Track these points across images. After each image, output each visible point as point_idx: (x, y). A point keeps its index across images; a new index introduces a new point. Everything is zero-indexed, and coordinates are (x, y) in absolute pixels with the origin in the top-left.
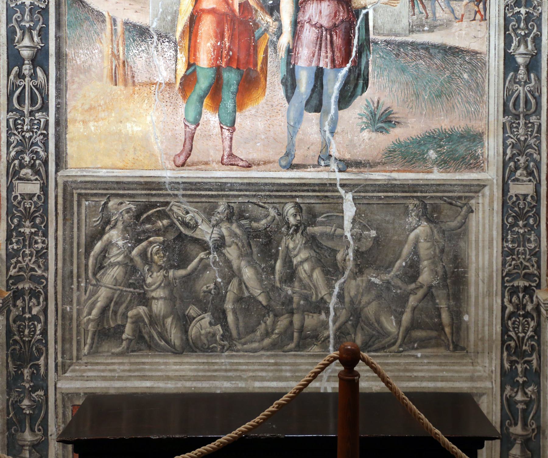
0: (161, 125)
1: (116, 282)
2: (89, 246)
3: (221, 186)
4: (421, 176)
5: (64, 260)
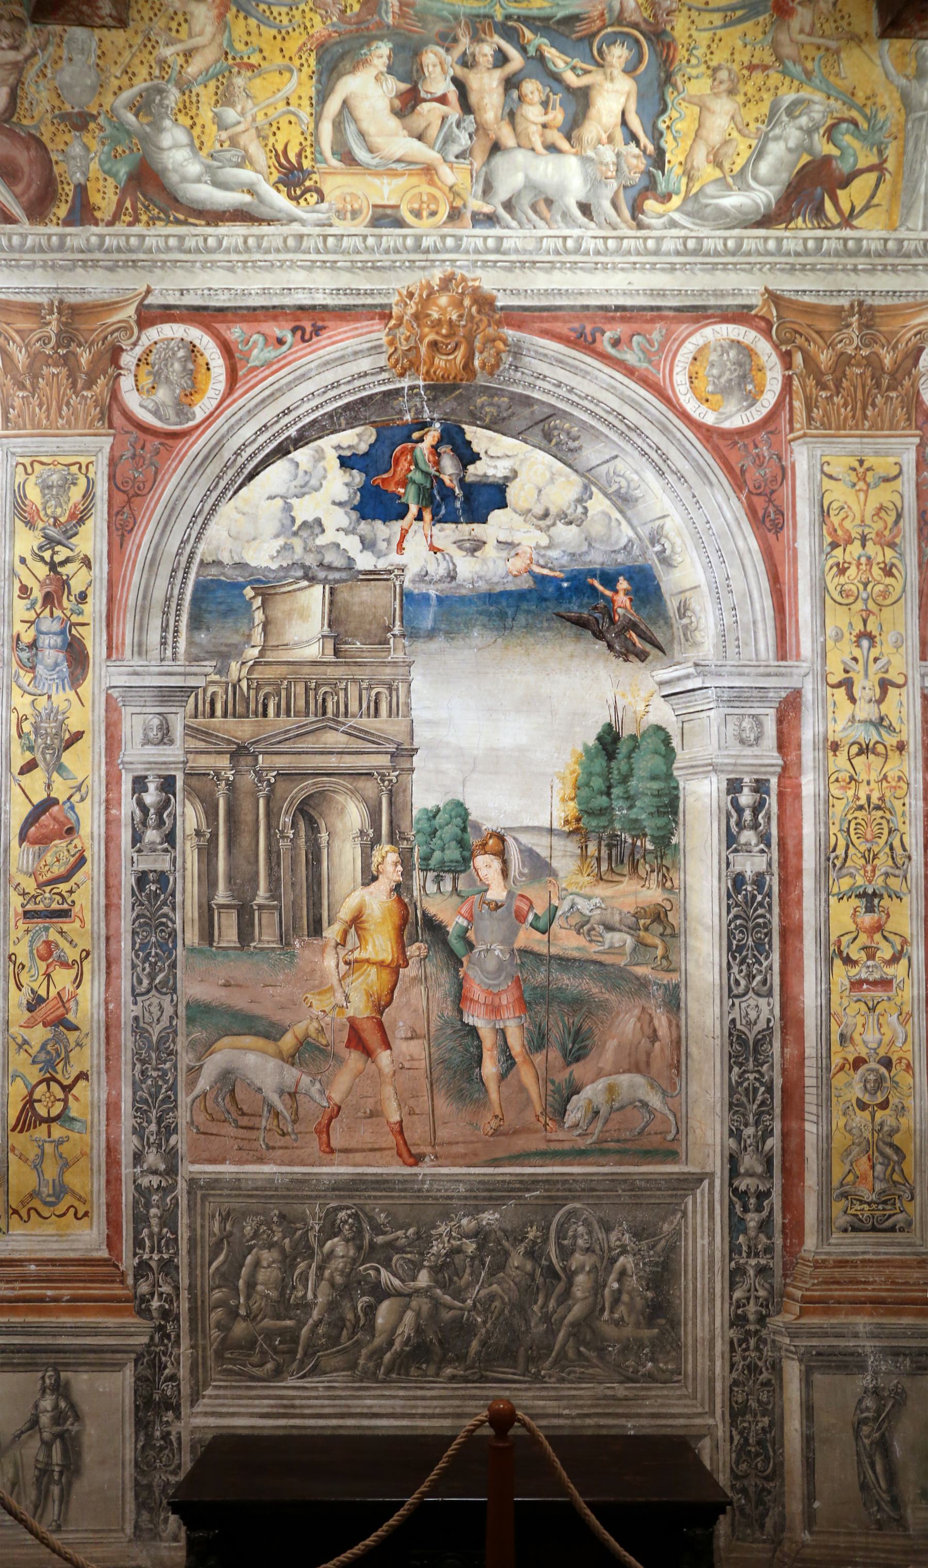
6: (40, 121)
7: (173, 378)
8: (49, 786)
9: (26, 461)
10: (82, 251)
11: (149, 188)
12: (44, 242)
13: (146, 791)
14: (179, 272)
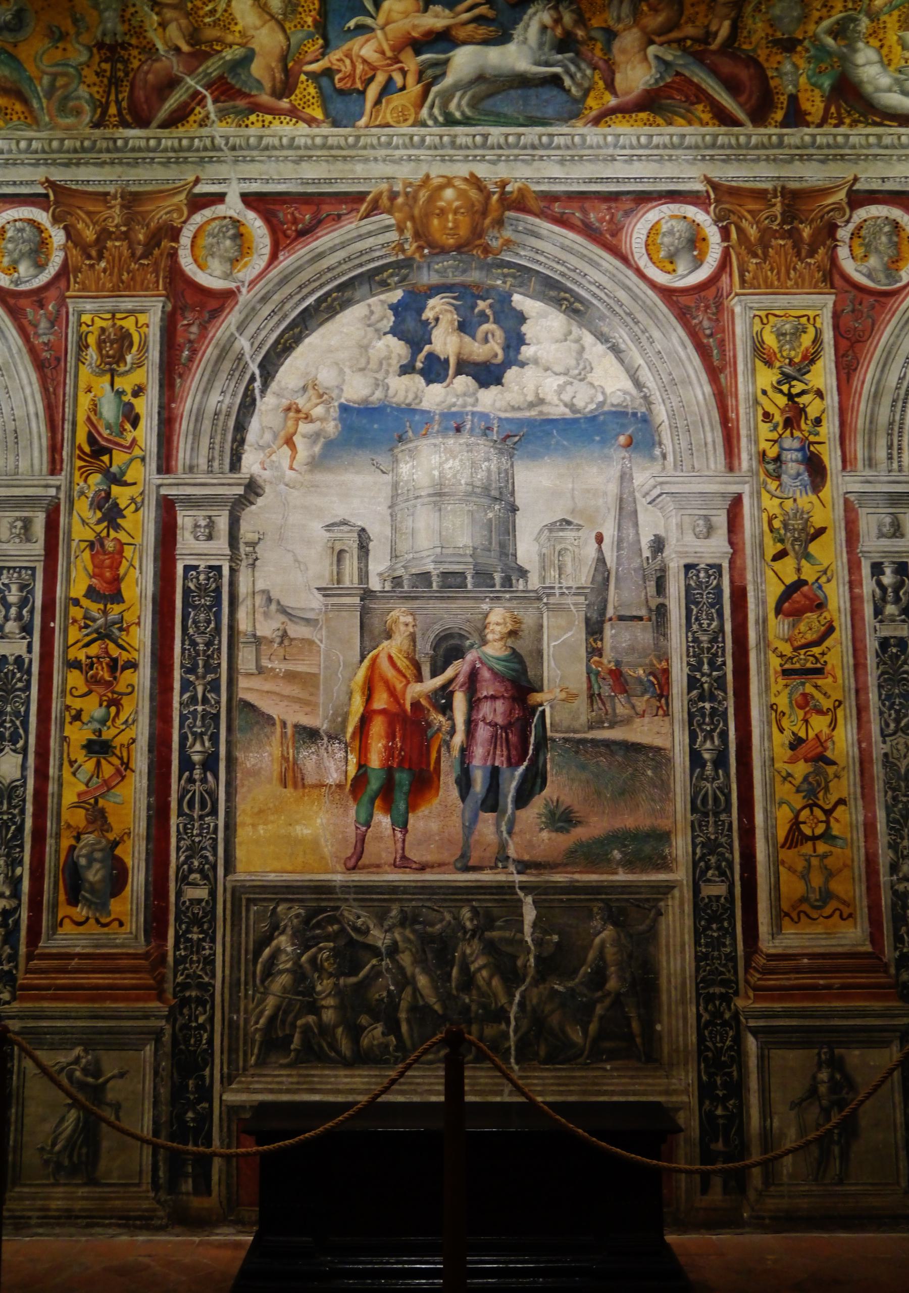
0: (331, 827)
1: (284, 989)
2: (257, 953)
3: (393, 889)
4: (604, 877)
5: (232, 967)
6: (757, 46)
7: (882, 248)
8: (799, 570)
9: (763, 314)
10: (798, 148)
11: (850, 99)
12: (765, 139)
13: (883, 573)
14: (880, 164)
